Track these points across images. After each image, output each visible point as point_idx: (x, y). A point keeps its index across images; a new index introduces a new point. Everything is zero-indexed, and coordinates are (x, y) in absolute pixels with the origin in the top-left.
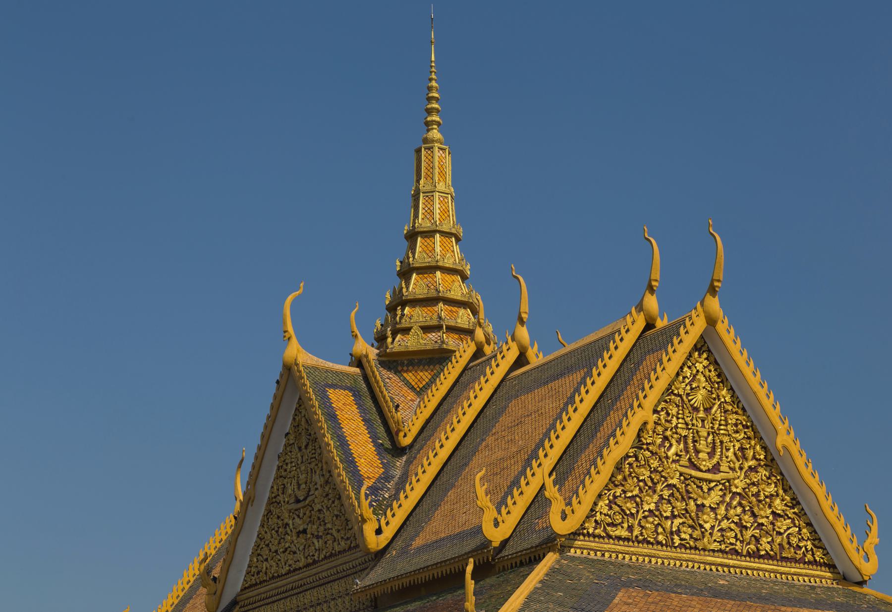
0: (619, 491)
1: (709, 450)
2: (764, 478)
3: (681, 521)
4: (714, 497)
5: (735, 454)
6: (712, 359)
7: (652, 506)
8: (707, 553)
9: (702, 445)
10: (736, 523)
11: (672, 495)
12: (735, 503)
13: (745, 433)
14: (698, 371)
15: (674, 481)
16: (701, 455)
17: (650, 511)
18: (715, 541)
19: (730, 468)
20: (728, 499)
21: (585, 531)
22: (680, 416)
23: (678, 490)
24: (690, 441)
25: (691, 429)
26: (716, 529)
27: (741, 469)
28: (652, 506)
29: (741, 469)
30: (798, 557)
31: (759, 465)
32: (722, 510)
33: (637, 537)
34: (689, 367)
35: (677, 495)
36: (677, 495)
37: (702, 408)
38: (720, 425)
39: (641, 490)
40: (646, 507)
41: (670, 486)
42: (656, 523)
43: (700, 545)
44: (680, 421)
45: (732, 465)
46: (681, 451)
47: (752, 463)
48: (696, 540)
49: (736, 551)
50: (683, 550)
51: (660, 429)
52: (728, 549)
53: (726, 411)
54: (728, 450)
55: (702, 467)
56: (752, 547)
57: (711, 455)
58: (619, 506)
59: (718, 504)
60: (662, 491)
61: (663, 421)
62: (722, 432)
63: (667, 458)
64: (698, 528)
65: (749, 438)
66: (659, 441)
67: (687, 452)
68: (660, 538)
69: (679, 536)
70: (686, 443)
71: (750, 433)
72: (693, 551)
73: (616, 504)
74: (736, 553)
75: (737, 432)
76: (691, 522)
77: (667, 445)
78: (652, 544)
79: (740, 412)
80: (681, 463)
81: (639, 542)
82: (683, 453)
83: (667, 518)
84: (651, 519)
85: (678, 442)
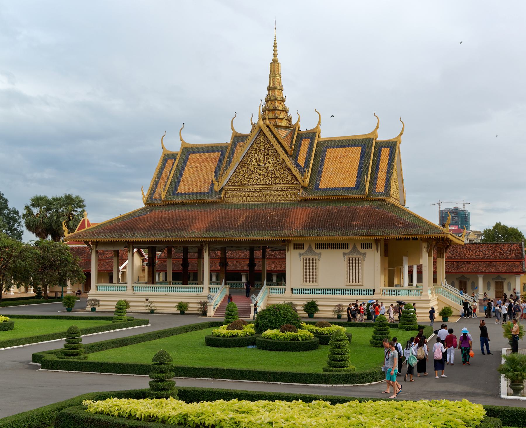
0: (238, 174)
3: (254, 179)
6: (265, 137)
10: (270, 177)
11: (252, 173)
12: (270, 172)
27: (272, 163)
28: (247, 177)
40: (245, 177)
41: (253, 171)
43: (260, 183)
47: (276, 161)
48: (258, 183)
53: (269, 150)
54: (269, 159)
57: (264, 161)
61: (251, 156)
63: (251, 164)
66: (249, 161)
67: (257, 162)
68: (249, 183)
74: (270, 184)
75: (272, 154)
76: (257, 178)
83: (251, 179)
85: (255, 160)
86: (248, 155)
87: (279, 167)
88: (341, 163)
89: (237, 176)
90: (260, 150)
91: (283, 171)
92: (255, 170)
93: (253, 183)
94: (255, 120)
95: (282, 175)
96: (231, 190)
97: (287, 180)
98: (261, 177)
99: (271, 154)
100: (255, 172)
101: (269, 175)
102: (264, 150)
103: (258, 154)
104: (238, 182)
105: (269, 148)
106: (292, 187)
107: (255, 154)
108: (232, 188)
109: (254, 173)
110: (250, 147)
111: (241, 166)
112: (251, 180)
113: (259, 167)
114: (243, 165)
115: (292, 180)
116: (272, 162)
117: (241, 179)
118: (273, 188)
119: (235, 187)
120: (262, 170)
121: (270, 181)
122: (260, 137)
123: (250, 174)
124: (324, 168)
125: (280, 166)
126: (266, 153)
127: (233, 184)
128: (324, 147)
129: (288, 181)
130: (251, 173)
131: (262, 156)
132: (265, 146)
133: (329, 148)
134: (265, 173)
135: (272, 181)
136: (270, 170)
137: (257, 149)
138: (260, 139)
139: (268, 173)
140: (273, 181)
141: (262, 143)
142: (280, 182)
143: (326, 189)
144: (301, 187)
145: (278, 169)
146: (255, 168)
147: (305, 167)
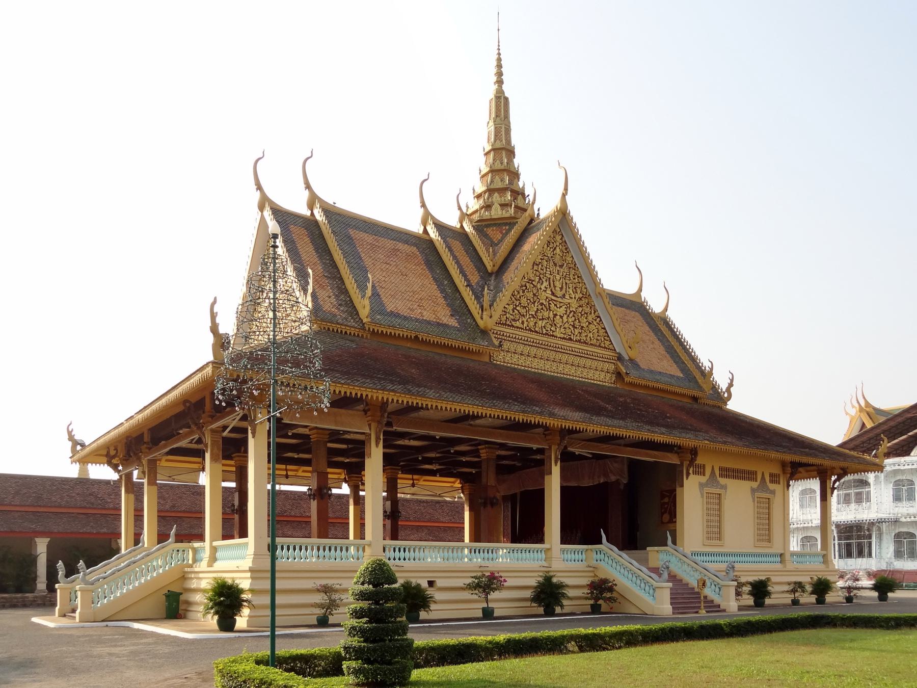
3: (546, 321)
4: (561, 311)
7: (534, 313)
9: (558, 285)
11: (542, 309)
16: (556, 289)
17: (532, 315)
18: (561, 333)
19: (570, 297)
20: (568, 313)
21: (502, 322)
22: (548, 267)
23: (544, 305)
26: (562, 328)
27: (575, 298)
28: (534, 313)
29: (575, 298)
31: (583, 297)
32: (565, 317)
34: (553, 243)
35: (544, 308)
36: (544, 308)
38: (566, 275)
40: (530, 313)
41: (542, 304)
42: (534, 321)
44: (548, 270)
45: (571, 296)
48: (553, 331)
49: (570, 338)
50: (547, 336)
51: (538, 274)
53: (570, 268)
57: (561, 289)
58: (517, 310)
59: (563, 314)
60: (537, 306)
61: (540, 269)
62: (567, 278)
63: (541, 289)
65: (579, 283)
67: (550, 286)
68: (537, 329)
69: (545, 328)
70: (549, 280)
71: (580, 281)
73: (516, 309)
74: (570, 339)
75: (574, 279)
77: (541, 282)
78: (533, 331)
80: (547, 292)
81: (526, 330)
84: (532, 319)
86: (535, 267)
89: (516, 306)
90: (555, 265)
91: (591, 319)
93: (544, 332)
96: (503, 335)
97: (597, 340)
102: (561, 266)
104: (518, 320)
108: (505, 330)
111: (522, 286)
114: (526, 286)
115: (605, 341)
118: (576, 350)
121: (571, 332)
123: (538, 310)
126: (565, 274)
127: (508, 323)
130: (540, 307)
131: (558, 277)
132: (562, 257)
135: (574, 335)
136: (571, 312)
137: (549, 260)
139: (568, 316)
140: (576, 336)
141: (558, 249)
142: (586, 340)
145: (583, 313)
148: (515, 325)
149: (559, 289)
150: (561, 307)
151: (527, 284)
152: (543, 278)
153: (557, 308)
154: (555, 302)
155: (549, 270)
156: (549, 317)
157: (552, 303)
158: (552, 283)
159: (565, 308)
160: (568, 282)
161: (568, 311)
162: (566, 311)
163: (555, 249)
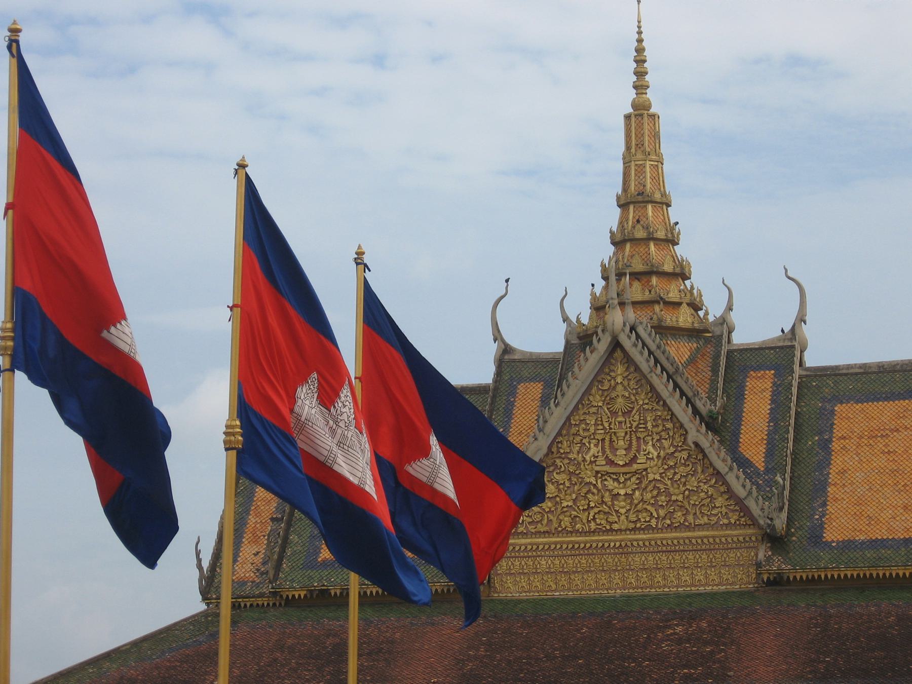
1: (626, 446)
2: (683, 461)
3: (596, 510)
5: (653, 445)
6: (632, 369)
8: (623, 533)
11: (589, 491)
12: (650, 488)
13: (664, 426)
14: (617, 383)
15: (593, 480)
17: (567, 506)
24: (607, 443)
25: (609, 432)
27: (658, 456)
28: (570, 504)
30: (713, 523)
33: (556, 529)
34: (609, 381)
37: (620, 413)
39: (559, 490)
40: (565, 504)
41: (590, 483)
43: (616, 526)
44: (601, 427)
45: (651, 456)
46: (598, 453)
47: (672, 450)
48: (611, 523)
51: (578, 439)
52: (643, 527)
54: (646, 443)
55: (618, 463)
56: (668, 522)
59: (634, 490)
63: (584, 460)
64: (614, 514)
67: (604, 452)
68: (578, 526)
71: (669, 425)
72: (610, 533)
74: (653, 529)
75: (657, 426)
79: (661, 408)
80: (598, 463)
82: (600, 454)
83: (584, 510)
85: (597, 446)
86: (574, 430)
87: (682, 470)
88: (889, 452)
90: (614, 414)
92: (599, 481)
94: (580, 310)
95: (694, 499)
98: (622, 505)
99: (653, 426)
100: (599, 485)
101: (648, 496)
103: (606, 425)
105: (646, 407)
106: (729, 540)
107: (596, 424)
109: (595, 491)
110: (580, 401)
112: (584, 516)
113: (608, 468)
115: (730, 514)
116: (656, 454)
117: (550, 512)
119: (529, 541)
120: (622, 479)
122: (612, 367)
124: (833, 471)
125: (685, 465)
126: (635, 424)
128: (823, 400)
129: (715, 519)
133: (841, 403)
134: (634, 490)
138: (612, 374)
140: (664, 518)
141: (620, 388)
143: (848, 545)
144: (760, 538)
146: (597, 472)
147: (767, 470)
148: (533, 531)
149: (624, 452)
150: (629, 479)
151: (558, 462)
152: (589, 443)
153: (620, 483)
154: (615, 477)
155: (601, 427)
156: (602, 501)
157: (609, 479)
158: (607, 443)
159: (638, 478)
160: (642, 436)
161: (645, 482)
162: (641, 482)
163: (614, 388)
